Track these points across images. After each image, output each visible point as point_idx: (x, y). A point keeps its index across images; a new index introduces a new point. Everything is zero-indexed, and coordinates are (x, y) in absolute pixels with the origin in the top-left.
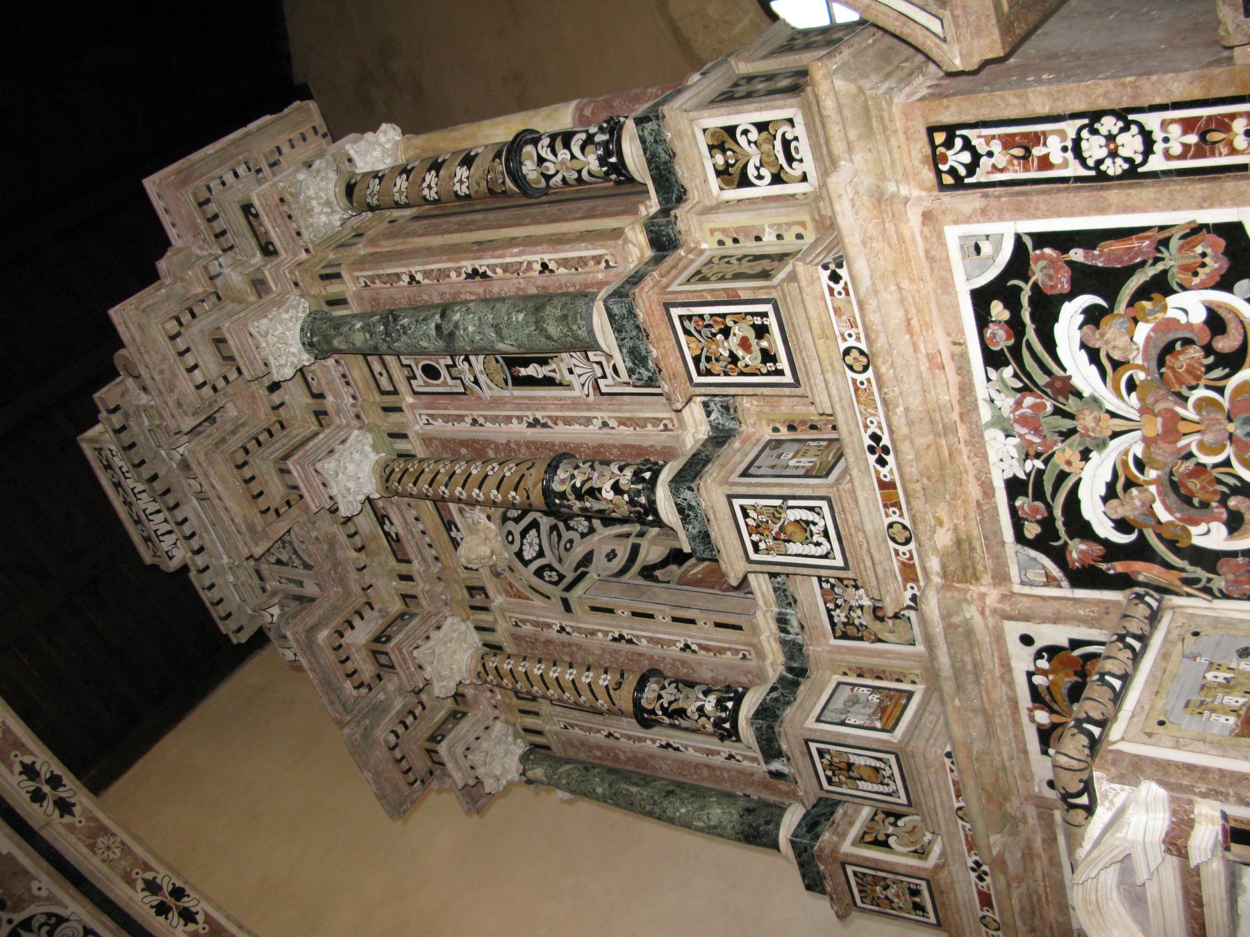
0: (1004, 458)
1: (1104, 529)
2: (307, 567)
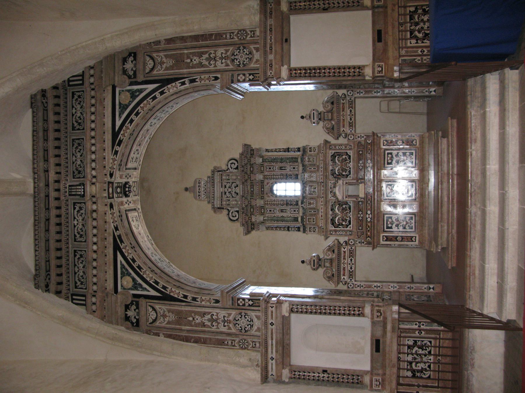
0: (331, 168)
1: (337, 173)
2: (233, 197)
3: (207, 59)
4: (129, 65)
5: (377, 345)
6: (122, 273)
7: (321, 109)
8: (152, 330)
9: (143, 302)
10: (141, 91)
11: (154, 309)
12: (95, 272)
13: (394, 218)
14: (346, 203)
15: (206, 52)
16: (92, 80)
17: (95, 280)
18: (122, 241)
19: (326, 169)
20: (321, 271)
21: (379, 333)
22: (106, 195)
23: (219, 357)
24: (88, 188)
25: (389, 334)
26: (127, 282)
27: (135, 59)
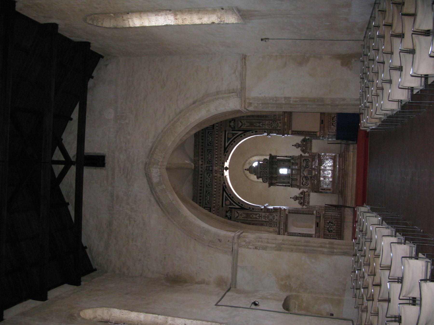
3: (262, 125)
4: (232, 124)
5: (317, 225)
6: (225, 199)
7: (300, 143)
8: (236, 220)
9: (233, 210)
10: (236, 134)
11: (237, 213)
12: (215, 199)
13: (324, 182)
14: (307, 177)
15: (261, 122)
16: (217, 128)
17: (214, 202)
18: (226, 188)
19: (301, 165)
20: (297, 201)
21: (318, 221)
22: (221, 170)
23: (263, 229)
24: (214, 168)
25: (321, 220)
26: (228, 203)
27: (234, 121)
